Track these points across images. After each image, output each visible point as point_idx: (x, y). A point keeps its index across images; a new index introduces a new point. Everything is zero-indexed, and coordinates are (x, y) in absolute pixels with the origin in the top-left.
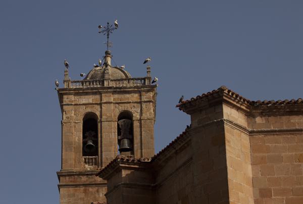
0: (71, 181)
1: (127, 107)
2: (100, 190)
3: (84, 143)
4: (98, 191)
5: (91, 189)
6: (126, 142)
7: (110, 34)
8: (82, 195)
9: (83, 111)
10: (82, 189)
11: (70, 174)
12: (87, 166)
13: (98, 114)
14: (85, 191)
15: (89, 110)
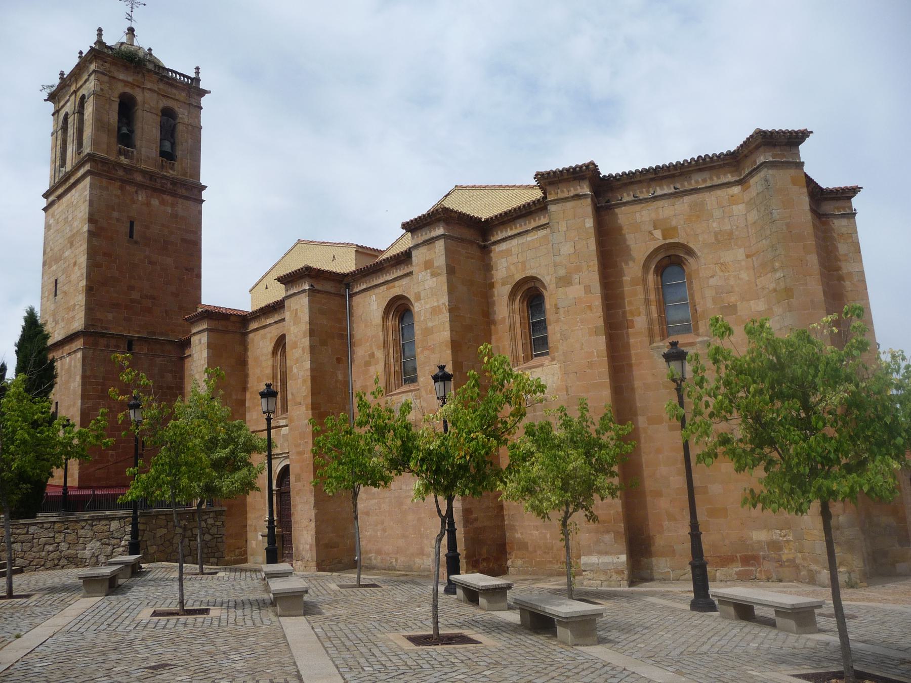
0: (104, 171)
1: (170, 103)
2: (139, 192)
3: (119, 129)
4: (136, 192)
5: (128, 188)
6: (167, 144)
7: (135, 7)
8: (119, 192)
9: (120, 88)
10: (118, 184)
11: (104, 162)
12: (122, 158)
13: (139, 98)
14: (122, 188)
15: (128, 90)
